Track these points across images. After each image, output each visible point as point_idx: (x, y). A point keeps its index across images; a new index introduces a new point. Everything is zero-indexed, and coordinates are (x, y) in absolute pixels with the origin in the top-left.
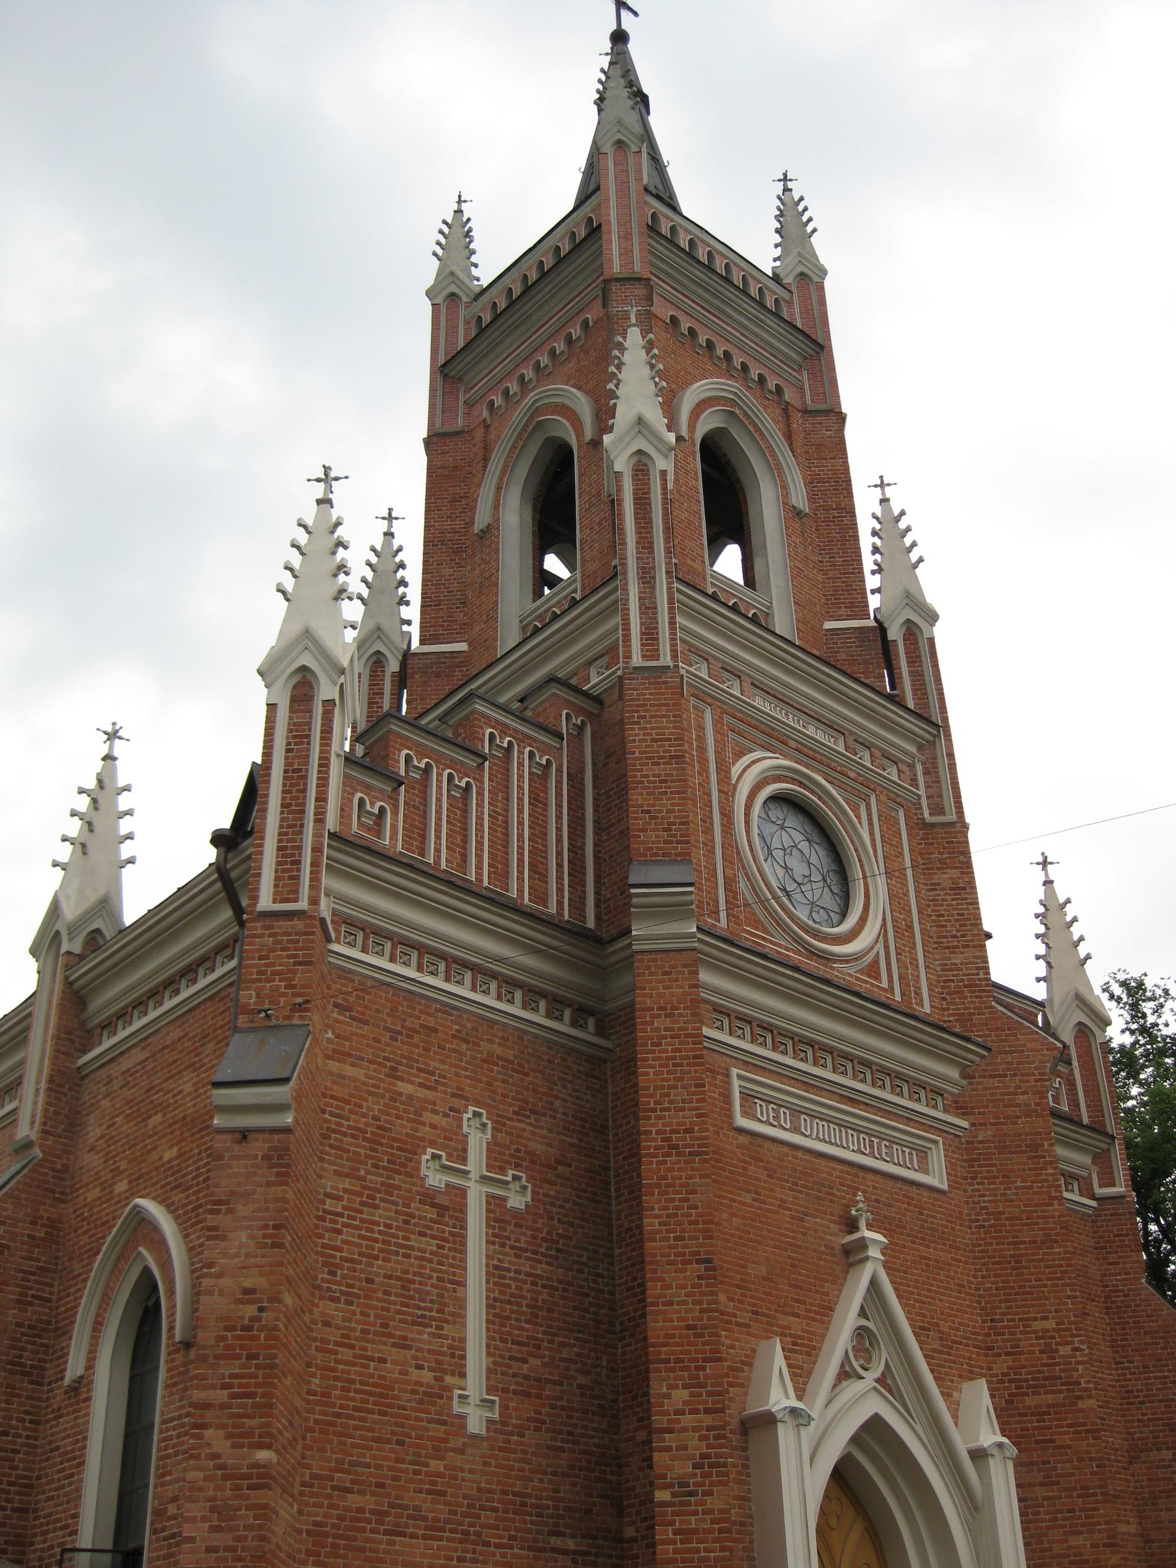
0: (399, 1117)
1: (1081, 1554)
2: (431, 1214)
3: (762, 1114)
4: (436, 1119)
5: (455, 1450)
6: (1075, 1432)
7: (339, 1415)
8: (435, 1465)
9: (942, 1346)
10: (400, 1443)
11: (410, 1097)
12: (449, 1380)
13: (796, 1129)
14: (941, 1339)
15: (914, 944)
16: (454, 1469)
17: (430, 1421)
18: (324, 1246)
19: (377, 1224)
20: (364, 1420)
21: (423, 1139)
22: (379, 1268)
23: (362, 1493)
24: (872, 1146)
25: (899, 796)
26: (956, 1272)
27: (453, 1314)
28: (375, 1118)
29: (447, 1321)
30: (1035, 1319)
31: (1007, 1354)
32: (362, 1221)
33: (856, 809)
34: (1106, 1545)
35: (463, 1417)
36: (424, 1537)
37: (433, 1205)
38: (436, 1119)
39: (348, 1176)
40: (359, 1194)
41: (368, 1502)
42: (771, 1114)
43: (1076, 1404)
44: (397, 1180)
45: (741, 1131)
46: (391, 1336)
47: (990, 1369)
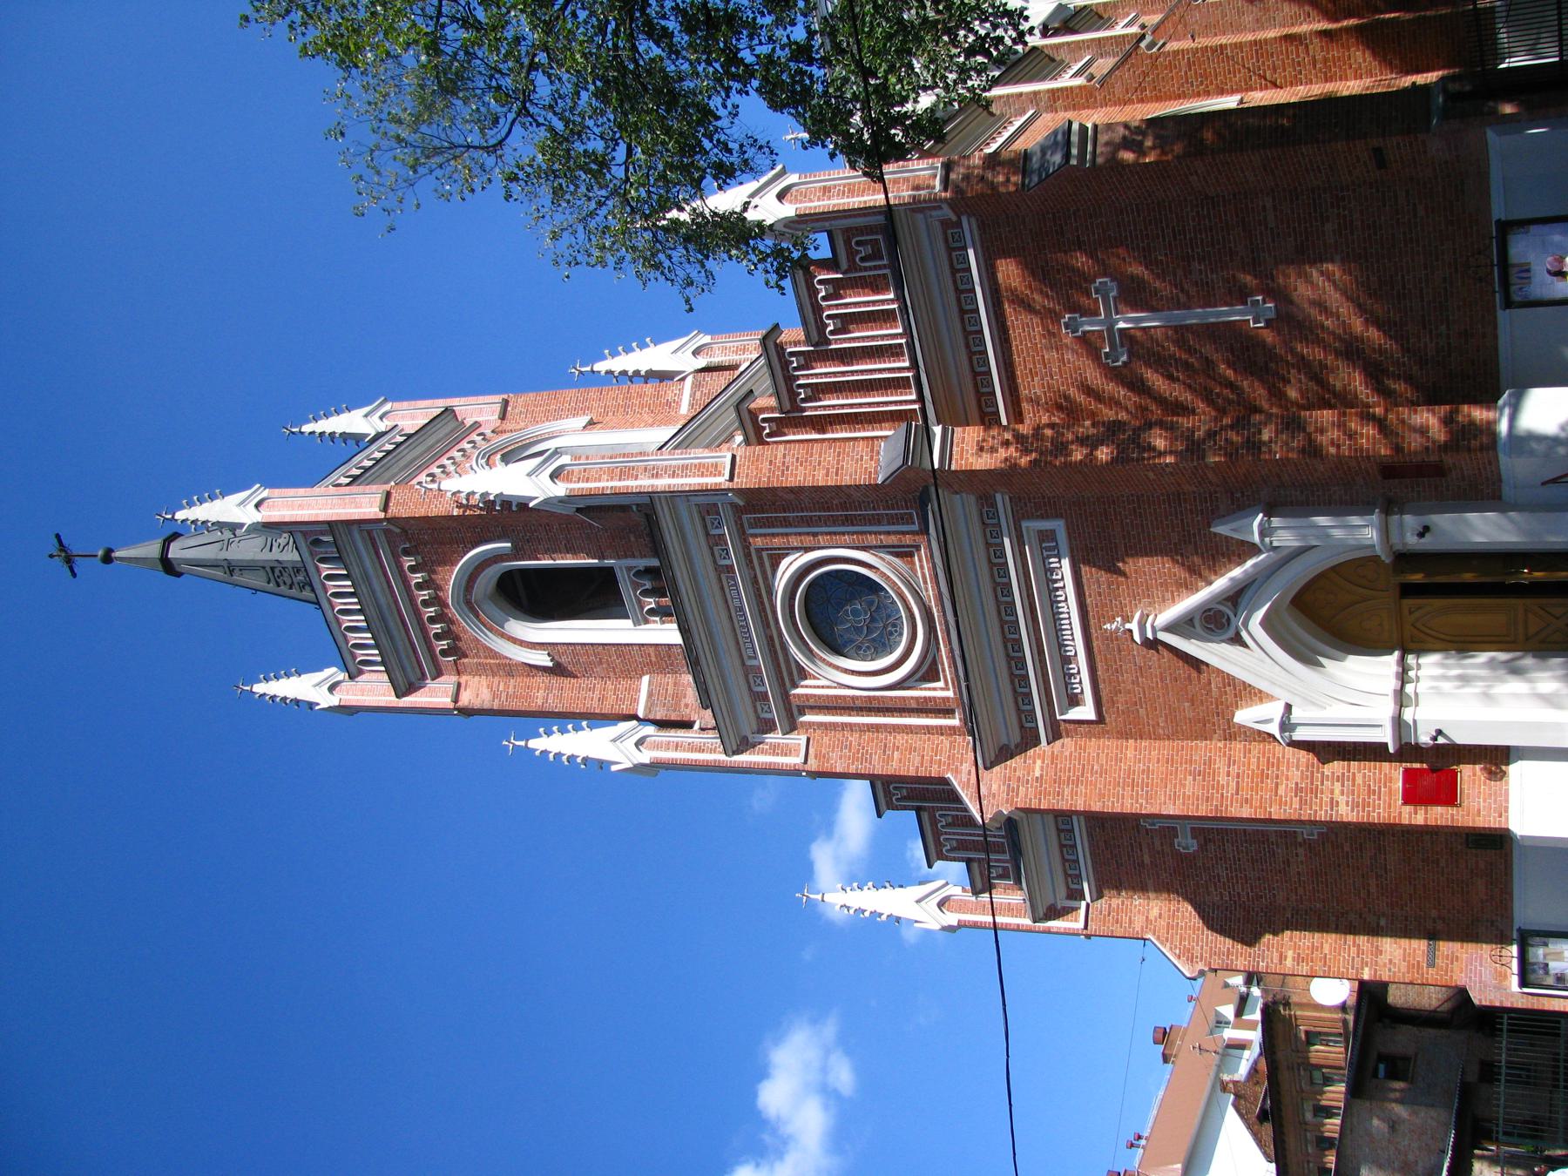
0: (1164, 863)
2: (1211, 847)
5: (1337, 837)
7: (1333, 895)
8: (1347, 849)
9: (1190, 542)
10: (1339, 866)
11: (1150, 857)
12: (1300, 839)
15: (860, 515)
17: (1324, 850)
18: (1248, 900)
19: (1227, 874)
21: (1172, 851)
23: (1369, 885)
25: (736, 522)
27: (1263, 835)
29: (1268, 840)
35: (1319, 834)
36: (1385, 854)
37: (1206, 845)
41: (1373, 882)
44: (1200, 864)
47: (1194, 492)
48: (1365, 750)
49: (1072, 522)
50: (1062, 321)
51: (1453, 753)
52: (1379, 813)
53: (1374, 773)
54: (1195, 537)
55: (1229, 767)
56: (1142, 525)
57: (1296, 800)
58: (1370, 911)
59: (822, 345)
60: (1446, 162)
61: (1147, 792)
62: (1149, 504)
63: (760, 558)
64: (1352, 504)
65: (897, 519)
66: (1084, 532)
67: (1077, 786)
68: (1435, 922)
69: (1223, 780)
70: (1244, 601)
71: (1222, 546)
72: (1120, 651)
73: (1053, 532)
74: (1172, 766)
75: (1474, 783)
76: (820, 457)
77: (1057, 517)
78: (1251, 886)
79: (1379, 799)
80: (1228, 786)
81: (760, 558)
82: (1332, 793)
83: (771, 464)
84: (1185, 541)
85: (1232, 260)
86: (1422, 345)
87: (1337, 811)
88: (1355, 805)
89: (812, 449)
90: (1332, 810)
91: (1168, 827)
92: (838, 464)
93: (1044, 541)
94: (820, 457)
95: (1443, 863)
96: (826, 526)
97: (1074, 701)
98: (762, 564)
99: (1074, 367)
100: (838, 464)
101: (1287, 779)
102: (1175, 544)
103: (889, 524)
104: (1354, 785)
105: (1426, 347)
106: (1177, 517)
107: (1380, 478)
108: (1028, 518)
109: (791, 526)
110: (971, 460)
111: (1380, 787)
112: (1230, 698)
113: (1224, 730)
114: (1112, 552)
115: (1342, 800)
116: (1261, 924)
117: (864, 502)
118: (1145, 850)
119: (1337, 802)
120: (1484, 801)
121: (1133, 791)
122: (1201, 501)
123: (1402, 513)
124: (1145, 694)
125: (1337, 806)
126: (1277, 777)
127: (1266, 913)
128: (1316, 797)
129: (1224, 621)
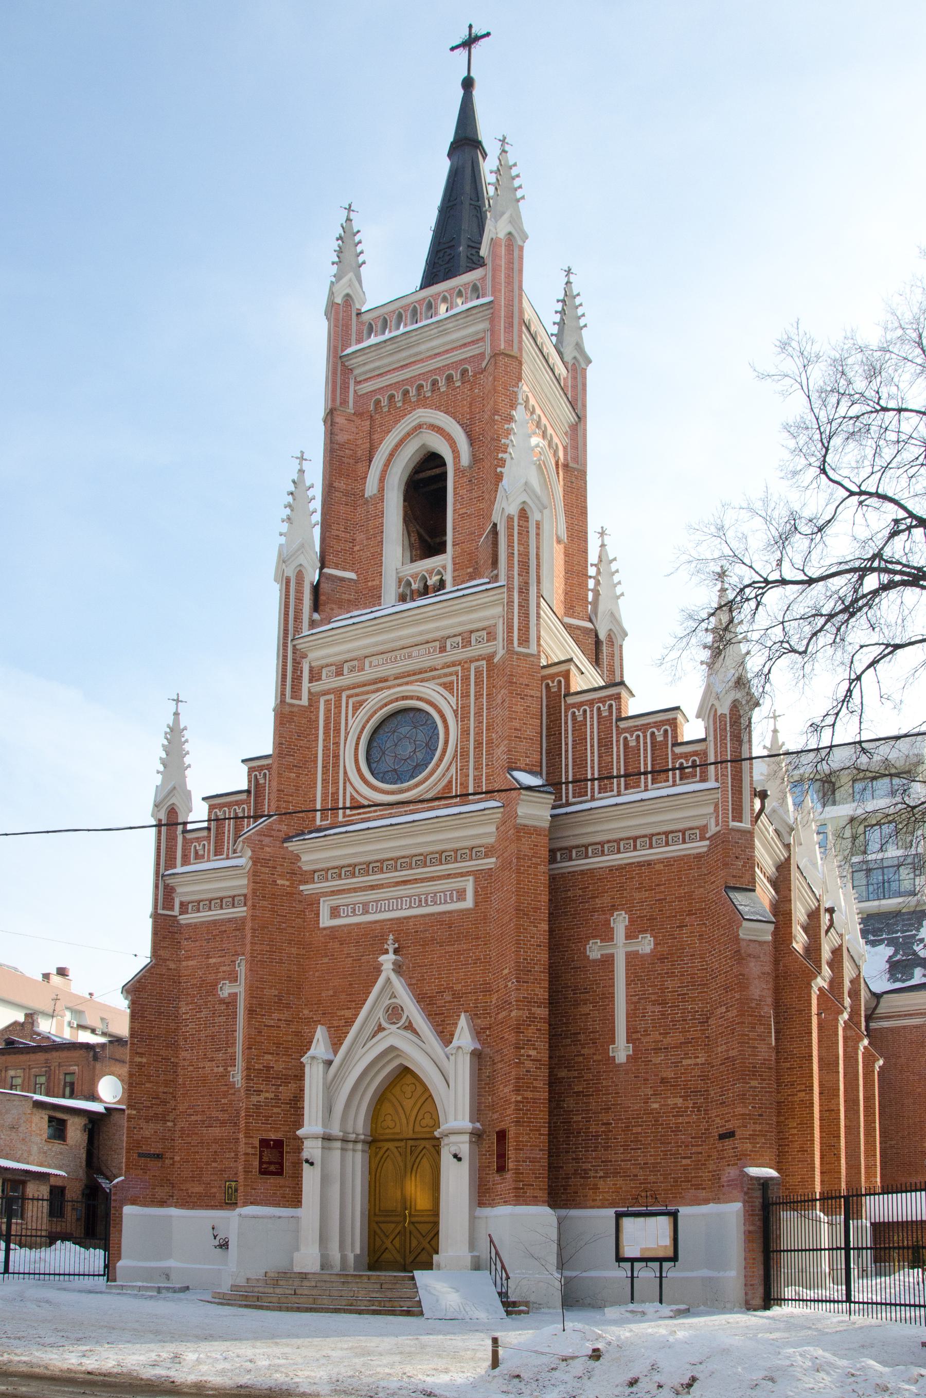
0: (209, 973)
1: (506, 1097)
2: (223, 1007)
3: (344, 912)
4: (224, 968)
5: (231, 1094)
6: (509, 1031)
10: (211, 1095)
11: (215, 963)
12: (229, 1069)
13: (366, 912)
15: (482, 754)
16: (231, 1101)
20: (197, 1090)
22: (203, 1034)
23: (197, 1115)
24: (420, 901)
26: (473, 953)
27: (232, 1043)
28: (201, 978)
30: (503, 969)
32: (197, 1018)
33: (448, 687)
34: (513, 1091)
37: (224, 1003)
38: (224, 968)
39: (191, 1004)
40: (194, 1009)
41: (199, 1118)
42: (350, 910)
43: (510, 1015)
45: (325, 929)
46: (207, 1058)
47: (491, 1002)
48: (299, 1115)
49: (472, 914)
50: (623, 912)
51: (295, 1173)
52: (252, 1123)
53: (281, 1121)
55: (284, 1021)
56: (467, 964)
57: (261, 1067)
58: (177, 1115)
59: (617, 730)
60: (720, 1179)
61: (266, 962)
62: (483, 970)
63: (451, 674)
64: (478, 1110)
65: (478, 783)
66: (463, 922)
67: (269, 911)
68: (170, 1158)
69: (276, 1016)
70: (408, 1034)
72: (372, 944)
73: (464, 899)
74: (285, 980)
75: (276, 1187)
76: (530, 725)
77: (476, 903)
78: (193, 1034)
79: (262, 1123)
80: (273, 1019)
81: (451, 674)
82: (267, 1091)
83: (526, 685)
84: (454, 994)
85: (660, 1034)
86: (590, 1160)
87: (253, 1095)
88: (257, 1106)
89: (536, 719)
90: (254, 1091)
91: (237, 977)
92: (524, 738)
93: (458, 892)
94: (530, 725)
95: (214, 1165)
96: (475, 728)
97: (335, 912)
98: (446, 675)
99: (588, 920)
100: (524, 738)
101: (276, 1061)
102: (453, 987)
103: (475, 776)
104: (272, 1106)
105: (589, 1162)
106: (471, 989)
107: (497, 1129)
108: (476, 882)
109: (476, 699)
110: (523, 840)
111: (271, 1124)
112: (335, 1023)
113: (313, 1018)
114: (448, 942)
115: (262, 1098)
116: (165, 1040)
117: (493, 757)
118: (219, 960)
119: (260, 1095)
120: (261, 1193)
121: (266, 951)
122: (483, 1006)
123: (471, 1142)
124: (339, 962)
125: (257, 1095)
126: (277, 1054)
127: (174, 1044)
128: (263, 1080)
129: (394, 1020)
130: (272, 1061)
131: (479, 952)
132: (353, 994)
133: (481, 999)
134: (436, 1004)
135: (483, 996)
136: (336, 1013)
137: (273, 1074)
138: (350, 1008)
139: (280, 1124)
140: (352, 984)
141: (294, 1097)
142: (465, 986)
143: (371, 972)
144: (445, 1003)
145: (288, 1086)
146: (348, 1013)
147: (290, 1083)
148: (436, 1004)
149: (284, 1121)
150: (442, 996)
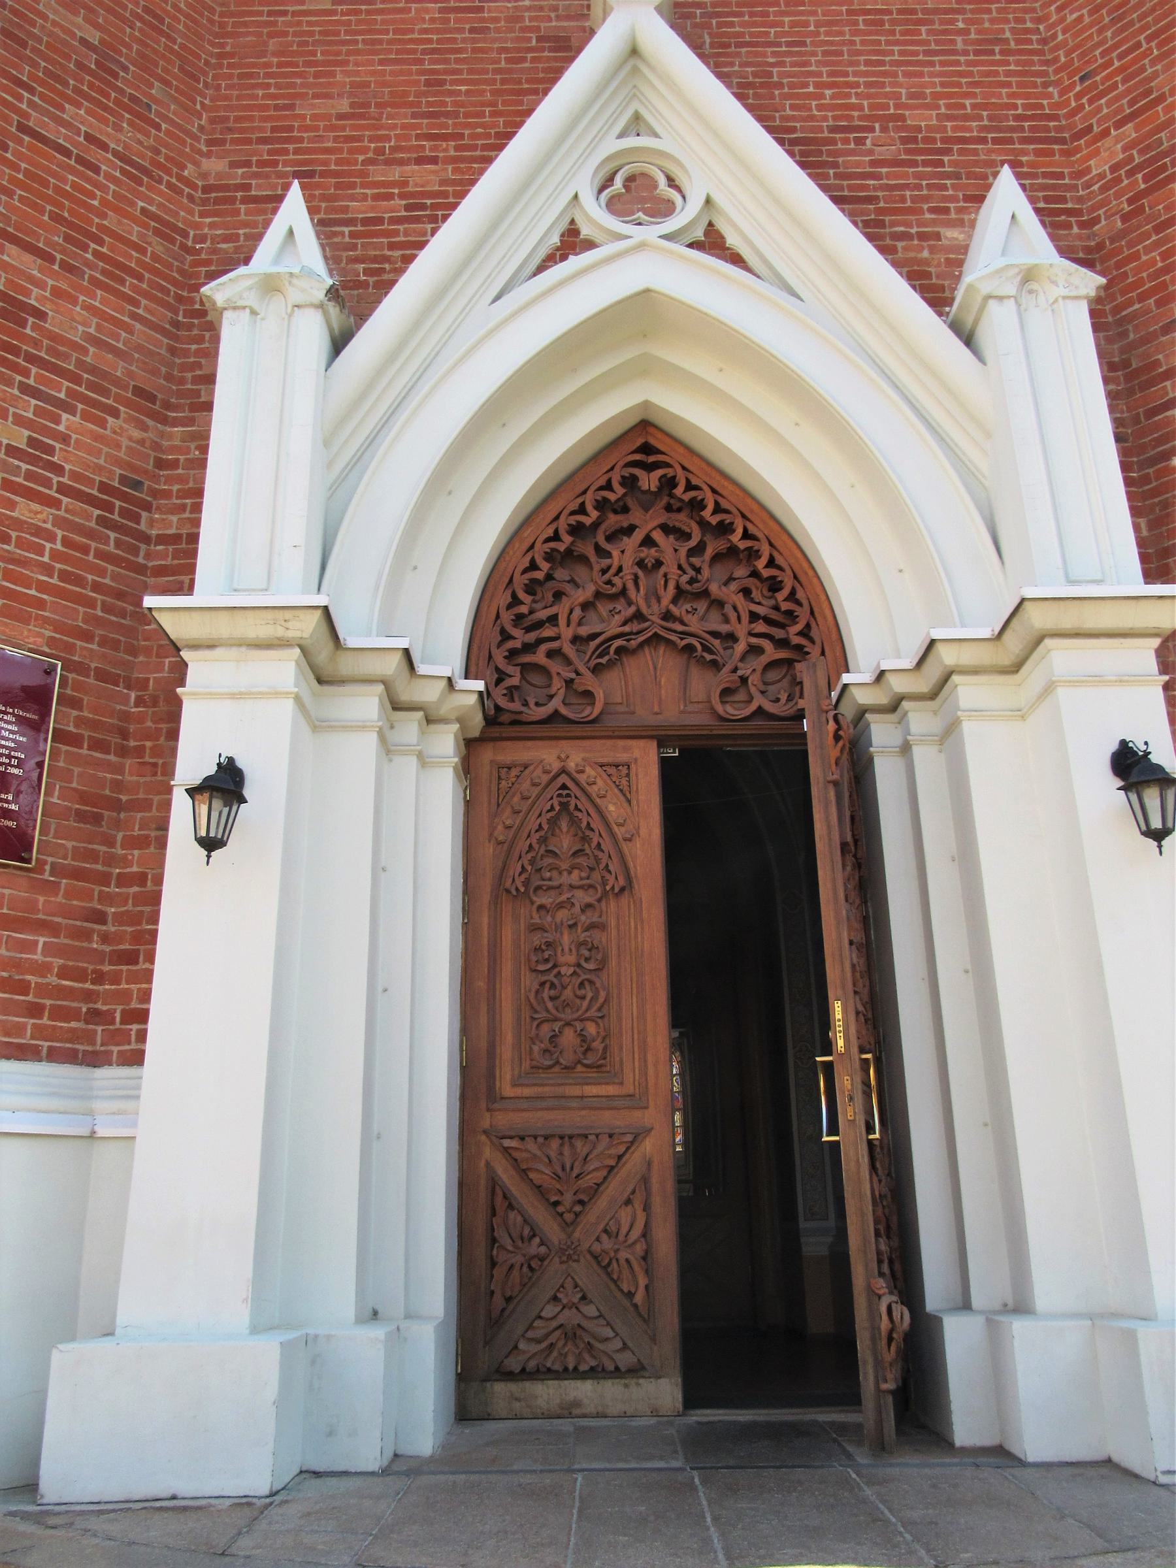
9: (908, 152)
14: (904, 141)
31: (1119, 125)
51: (93, 856)
53: (48, 569)
54: (926, 163)
71: (908, 224)
106: (982, 129)
113: (246, 187)
130: (41, 285)
131: (992, 21)
132: (447, 115)
133: (1031, 165)
134: (835, 165)
135: (1038, 152)
136: (363, 174)
137: (36, 344)
138: (434, 160)
139: (42, 587)
140: (442, 83)
141: (123, 480)
142: (949, 118)
143: (530, 50)
144: (873, 163)
145: (102, 424)
146: (423, 178)
147: (115, 414)
148: (835, 165)
149: (64, 576)
150: (860, 141)
